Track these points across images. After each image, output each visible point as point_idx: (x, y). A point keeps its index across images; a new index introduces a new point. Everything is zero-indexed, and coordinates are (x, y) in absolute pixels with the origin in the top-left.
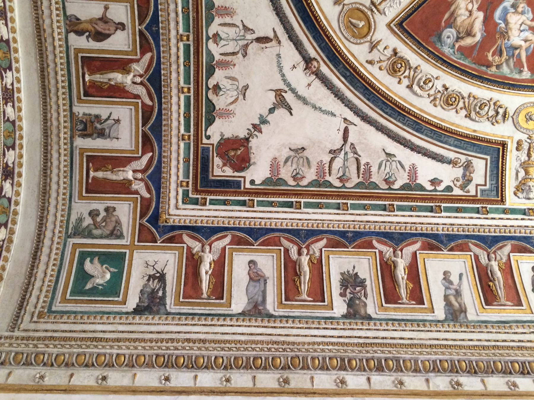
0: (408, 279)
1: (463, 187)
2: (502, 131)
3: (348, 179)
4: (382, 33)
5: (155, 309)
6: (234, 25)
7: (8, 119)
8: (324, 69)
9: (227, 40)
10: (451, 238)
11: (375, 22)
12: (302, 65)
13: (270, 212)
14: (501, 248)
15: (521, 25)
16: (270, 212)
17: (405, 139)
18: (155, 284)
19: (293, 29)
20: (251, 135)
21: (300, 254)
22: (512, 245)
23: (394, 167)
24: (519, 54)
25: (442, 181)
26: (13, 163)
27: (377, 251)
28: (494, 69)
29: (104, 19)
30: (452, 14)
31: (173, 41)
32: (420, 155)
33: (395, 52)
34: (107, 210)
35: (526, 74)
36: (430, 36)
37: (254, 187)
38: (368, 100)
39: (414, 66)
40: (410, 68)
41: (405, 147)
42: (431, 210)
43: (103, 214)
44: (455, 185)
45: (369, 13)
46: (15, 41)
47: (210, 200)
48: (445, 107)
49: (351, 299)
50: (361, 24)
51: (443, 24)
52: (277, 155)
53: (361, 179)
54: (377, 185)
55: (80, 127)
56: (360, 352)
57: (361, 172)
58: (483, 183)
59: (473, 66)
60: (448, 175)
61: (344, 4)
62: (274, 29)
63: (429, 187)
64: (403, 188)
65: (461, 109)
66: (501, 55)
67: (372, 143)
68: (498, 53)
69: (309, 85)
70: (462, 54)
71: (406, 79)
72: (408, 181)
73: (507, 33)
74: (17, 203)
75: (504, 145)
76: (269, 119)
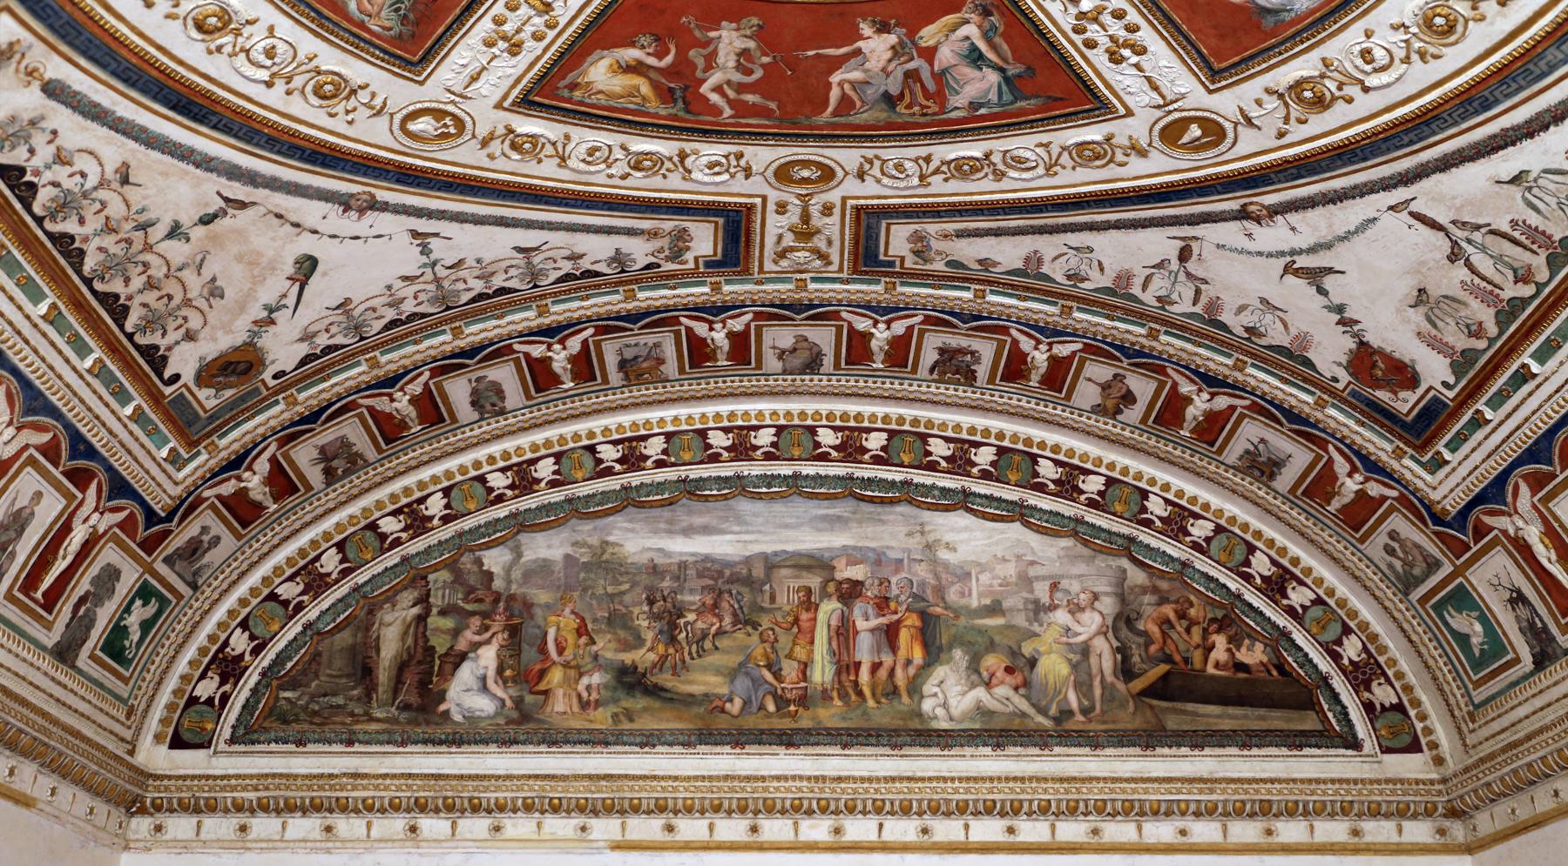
4: (1225, 104)
5: (1550, 650)
6: (1148, 280)
7: (1208, 540)
8: (1271, 199)
9: (1172, 292)
12: (1250, 225)
13: (1514, 410)
16: (1514, 410)
17: (1494, 136)
18: (1524, 612)
20: (1355, 335)
23: (1552, 186)
26: (1274, 562)
29: (1105, 387)
31: (1154, 344)
32: (1552, 128)
34: (1392, 538)
36: (1259, 26)
37: (1457, 390)
38: (1365, 159)
39: (1320, 65)
40: (1322, 76)
43: (1396, 545)
45: (1177, 115)
46: (1111, 466)
47: (1446, 446)
50: (1195, 131)
52: (1413, 327)
53: (1543, 254)
55: (1257, 473)
57: (1527, 242)
67: (1468, 189)
69: (1293, 229)
74: (1331, 592)
76: (1337, 301)
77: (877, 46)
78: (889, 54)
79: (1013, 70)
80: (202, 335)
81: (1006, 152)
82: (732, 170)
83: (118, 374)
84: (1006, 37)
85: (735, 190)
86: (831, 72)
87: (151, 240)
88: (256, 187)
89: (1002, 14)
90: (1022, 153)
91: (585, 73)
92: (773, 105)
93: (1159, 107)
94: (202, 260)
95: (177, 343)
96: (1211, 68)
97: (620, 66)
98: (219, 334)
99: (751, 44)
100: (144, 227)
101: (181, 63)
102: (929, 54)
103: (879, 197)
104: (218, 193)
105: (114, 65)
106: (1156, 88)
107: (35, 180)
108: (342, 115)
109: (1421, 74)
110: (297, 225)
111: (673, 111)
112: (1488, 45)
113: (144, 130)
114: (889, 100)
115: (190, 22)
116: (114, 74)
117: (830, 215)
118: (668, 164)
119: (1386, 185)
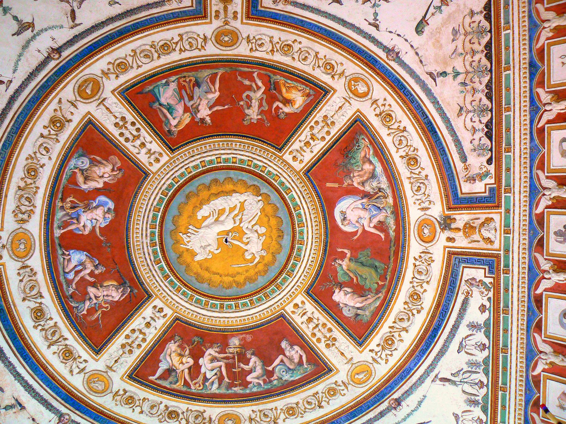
8: (52, 64)
11: (91, 102)
12: (55, 46)
15: (96, 219)
19: (82, 38)
28: (60, 204)
30: (100, 163)
35: (58, 233)
36: (82, 147)
38: (29, 101)
39: (58, 138)
40: (57, 135)
45: (97, 97)
48: (26, 168)
51: (92, 157)
59: (62, 187)
61: (102, 77)
62: (82, 24)
65: (25, 182)
66: (73, 208)
68: (73, 205)
69: (39, 51)
71: (48, 133)
73: (89, 209)
77: (204, 113)
78: (200, 107)
79: (156, 105)
80: (468, 11)
81: (153, 60)
82: (254, 41)
83: (502, 15)
84: (161, 121)
85: (254, 28)
86: (219, 97)
87: (464, 75)
88: (424, 81)
89: (164, 132)
90: (147, 60)
91: (304, 101)
92: (239, 78)
93: (104, 99)
94: (453, 54)
95: (477, 13)
97: (292, 103)
98: (462, 6)
99: (247, 111)
100: (464, 84)
101: (427, 149)
102: (186, 109)
103: (197, 24)
104: (436, 86)
105: (445, 158)
106: (107, 108)
107: (484, 127)
108: (387, 104)
110: (417, 54)
111: (275, 77)
113: (447, 128)
114: (197, 84)
115: (419, 164)
116: (446, 155)
117: (217, 12)
118: (278, 46)
119: (18, 92)
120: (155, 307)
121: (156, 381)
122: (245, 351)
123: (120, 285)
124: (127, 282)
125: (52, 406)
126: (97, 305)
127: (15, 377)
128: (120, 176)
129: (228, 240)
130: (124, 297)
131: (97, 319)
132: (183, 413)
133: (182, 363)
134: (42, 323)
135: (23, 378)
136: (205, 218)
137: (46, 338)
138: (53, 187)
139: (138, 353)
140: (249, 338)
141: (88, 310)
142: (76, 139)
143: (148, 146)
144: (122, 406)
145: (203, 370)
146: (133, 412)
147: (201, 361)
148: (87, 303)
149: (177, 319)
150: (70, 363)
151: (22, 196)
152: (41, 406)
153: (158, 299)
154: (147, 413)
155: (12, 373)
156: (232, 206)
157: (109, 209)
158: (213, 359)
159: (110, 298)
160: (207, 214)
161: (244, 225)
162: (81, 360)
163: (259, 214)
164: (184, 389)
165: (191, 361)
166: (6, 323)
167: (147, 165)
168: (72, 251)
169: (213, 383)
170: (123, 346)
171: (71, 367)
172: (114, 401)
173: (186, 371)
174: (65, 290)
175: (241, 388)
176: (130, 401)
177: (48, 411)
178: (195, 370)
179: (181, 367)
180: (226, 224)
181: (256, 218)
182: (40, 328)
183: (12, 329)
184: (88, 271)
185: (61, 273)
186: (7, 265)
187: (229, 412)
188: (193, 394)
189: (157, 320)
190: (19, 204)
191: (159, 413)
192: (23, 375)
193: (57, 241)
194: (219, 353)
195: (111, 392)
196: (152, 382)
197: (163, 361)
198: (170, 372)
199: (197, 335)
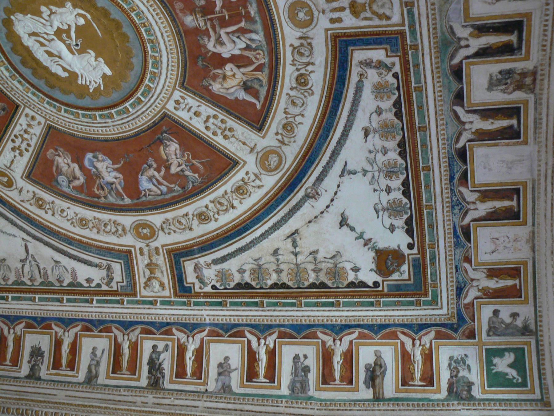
0: (70, 352)
1: (108, 284)
2: (128, 240)
3: (35, 280)
4: (21, 183)
10: (101, 322)
14: (133, 330)
15: (107, 168)
21: (9, 333)
22: (141, 328)
23: (61, 270)
24: (116, 187)
25: (93, 280)
27: (54, 331)
30: (57, 167)
33: (34, 194)
35: (127, 201)
38: (32, 225)
39: (51, 202)
41: (65, 255)
42: (87, 301)
44: (103, 283)
45: (7, 172)
49: (34, 366)
50: (6, 179)
53: (43, 280)
54: (53, 284)
56: (14, 404)
58: (121, 281)
59: (88, 198)
60: (98, 276)
63: (86, 285)
64: (69, 285)
65: (93, 227)
66: (103, 189)
67: (44, 254)
70: (78, 191)
72: (72, 280)
73: (100, 174)
75: (130, 252)
96: (29, 174)
109: (67, 225)
112: (86, 235)
119: (29, 234)
120: (175, 108)
121: (262, 102)
122: (199, 8)
123: (163, 144)
124: (157, 137)
125: (297, 205)
126: (187, 164)
127: (265, 238)
128: (62, 149)
129: (74, 43)
130: (174, 139)
131: (201, 163)
132: (298, 70)
133: (234, 75)
134: (211, 214)
135: (266, 231)
136: (65, 70)
137: (226, 210)
138: (91, 206)
139: (231, 122)
140: (179, 6)
141: (194, 172)
142: (45, 187)
143: (25, 127)
144: (295, 136)
145: (237, 52)
146: (302, 123)
147: (226, 55)
148: (187, 173)
149: (182, 85)
150: (250, 189)
151: (104, 230)
152: (296, 215)
153: (167, 106)
154: (302, 109)
155: (261, 241)
156: (38, 45)
157: (94, 157)
158: (219, 42)
159: (178, 152)
160: (61, 69)
161: (51, 31)
162: (246, 178)
163: (29, 15)
164: (266, 71)
165: (229, 67)
166: (213, 245)
167: (42, 126)
168: (141, 189)
169: (250, 40)
170: (226, 137)
171: (254, 187)
172: (291, 144)
173: (242, 70)
174: (177, 194)
175: (249, 6)
176: (289, 128)
177: (301, 209)
178: (239, 61)
179: (239, 76)
180: (58, 50)
181: (37, 18)
182: (216, 216)
183: (220, 240)
184: (156, 173)
185: (162, 197)
186: (163, 244)
187: (287, 17)
188: (271, 60)
189: (190, 106)
190: (111, 233)
191: (302, 96)
192: (263, 231)
193: (135, 201)
194: (209, 37)
195: (280, 147)
196: (263, 106)
197: (235, 96)
198: (246, 87)
199: (196, 63)
